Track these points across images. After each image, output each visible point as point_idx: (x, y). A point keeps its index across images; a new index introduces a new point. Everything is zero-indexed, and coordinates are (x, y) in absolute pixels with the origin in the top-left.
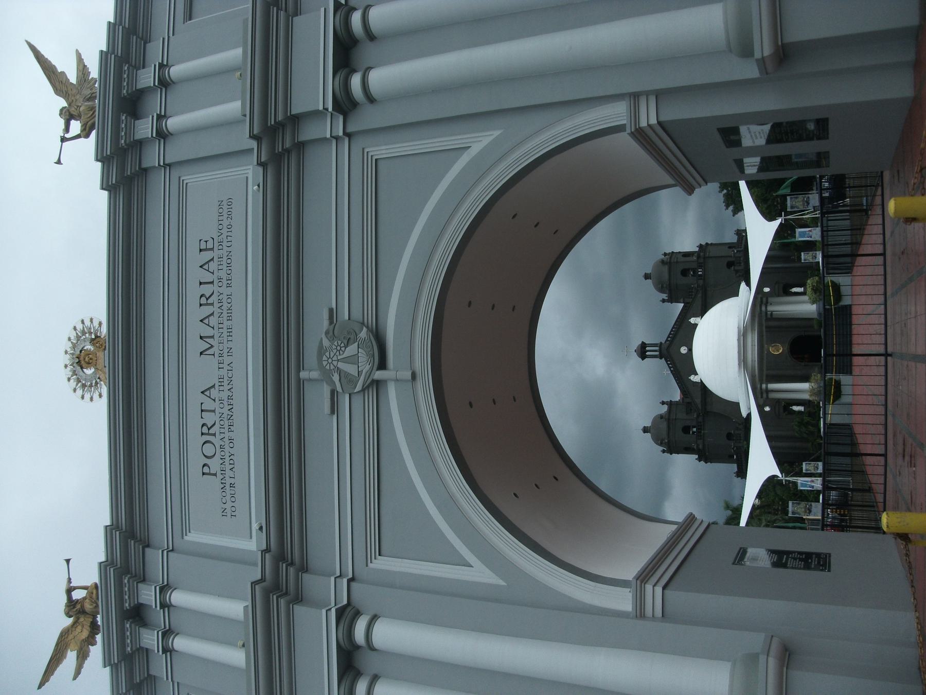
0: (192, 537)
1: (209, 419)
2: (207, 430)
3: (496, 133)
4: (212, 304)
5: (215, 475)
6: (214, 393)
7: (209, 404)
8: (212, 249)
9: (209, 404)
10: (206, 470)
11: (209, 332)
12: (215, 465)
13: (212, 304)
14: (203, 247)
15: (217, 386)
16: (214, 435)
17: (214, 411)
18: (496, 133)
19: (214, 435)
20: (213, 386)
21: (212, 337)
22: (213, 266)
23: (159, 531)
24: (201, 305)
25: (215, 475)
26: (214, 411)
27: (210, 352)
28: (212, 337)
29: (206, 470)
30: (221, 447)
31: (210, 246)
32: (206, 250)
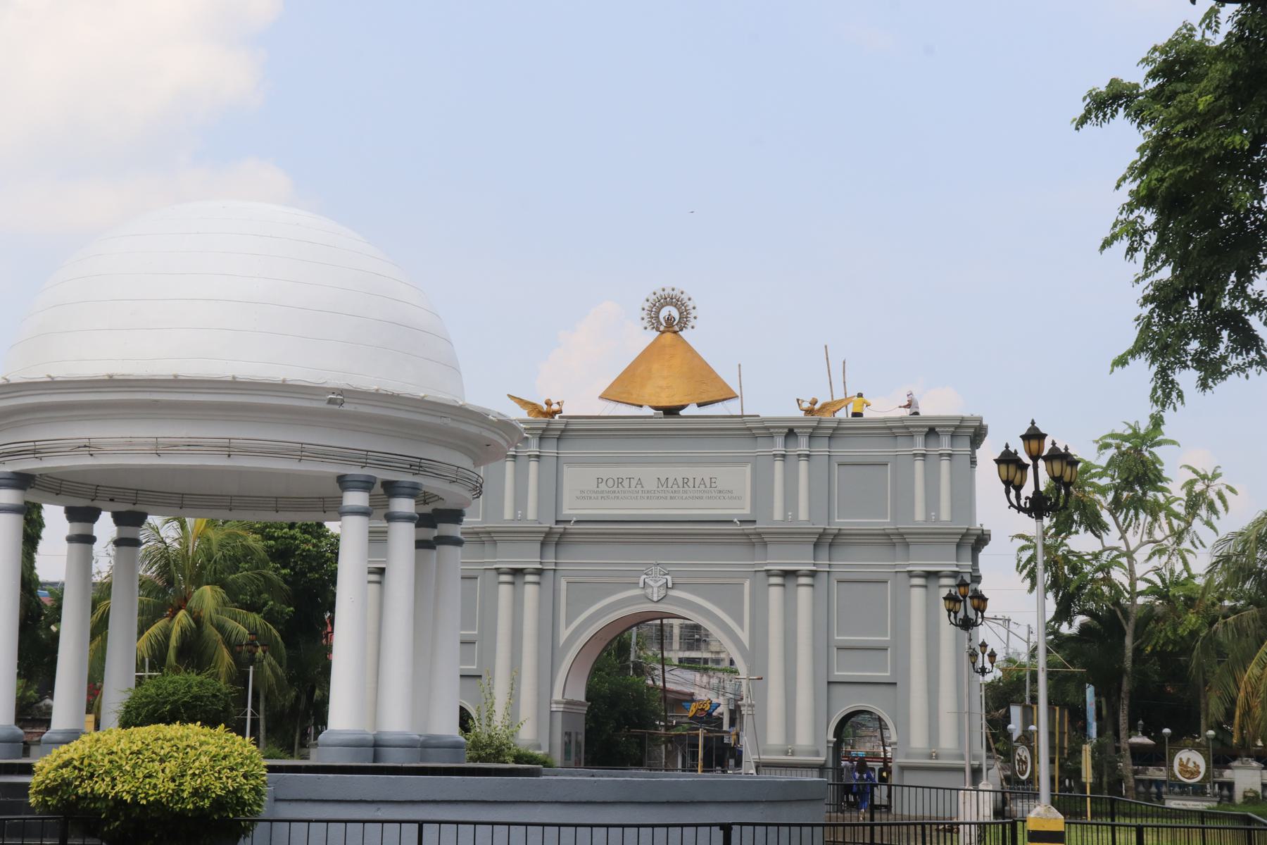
0: (565, 466)
1: (626, 483)
2: (620, 482)
3: (747, 646)
4: (683, 487)
5: (598, 487)
6: (639, 486)
7: (634, 483)
8: (711, 487)
9: (634, 483)
10: (600, 480)
11: (670, 485)
12: (603, 487)
13: (683, 487)
14: (713, 480)
15: (642, 489)
16: (618, 487)
17: (630, 487)
18: (747, 646)
19: (618, 487)
20: (642, 487)
21: (667, 487)
22: (702, 486)
23: (568, 451)
24: (683, 479)
25: (598, 487)
26: (630, 487)
27: (660, 485)
28: (667, 487)
29: (600, 480)
30: (614, 492)
31: (713, 485)
32: (711, 482)
